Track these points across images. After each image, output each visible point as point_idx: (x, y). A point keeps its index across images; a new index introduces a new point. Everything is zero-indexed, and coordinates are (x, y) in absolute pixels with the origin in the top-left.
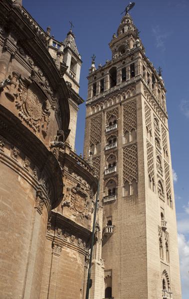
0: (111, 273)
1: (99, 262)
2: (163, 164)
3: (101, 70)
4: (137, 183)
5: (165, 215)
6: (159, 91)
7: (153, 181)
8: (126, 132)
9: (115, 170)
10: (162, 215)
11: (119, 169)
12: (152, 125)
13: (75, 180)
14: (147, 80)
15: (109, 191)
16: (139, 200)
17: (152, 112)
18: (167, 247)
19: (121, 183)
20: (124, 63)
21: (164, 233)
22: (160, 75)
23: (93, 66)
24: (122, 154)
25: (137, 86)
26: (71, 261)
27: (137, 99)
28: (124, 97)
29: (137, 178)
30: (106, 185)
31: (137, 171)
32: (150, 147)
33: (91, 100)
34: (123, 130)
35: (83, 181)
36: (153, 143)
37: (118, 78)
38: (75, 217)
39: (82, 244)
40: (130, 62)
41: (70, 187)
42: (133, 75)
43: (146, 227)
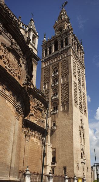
0: (55, 150)
1: (49, 145)
3: (49, 42)
4: (68, 104)
5: (83, 120)
6: (81, 54)
7: (77, 103)
8: (63, 77)
10: (81, 120)
11: (59, 96)
12: (77, 73)
13: (36, 102)
14: (74, 47)
15: (54, 108)
16: (70, 112)
17: (77, 65)
18: (84, 136)
19: (60, 104)
20: (62, 37)
21: (82, 130)
22: (81, 44)
23: (45, 39)
24: (61, 88)
25: (69, 51)
26: (35, 144)
27: (69, 58)
28: (62, 57)
29: (69, 101)
30: (53, 105)
31: (69, 97)
32: (75, 84)
33: (44, 59)
35: (40, 103)
36: (77, 82)
37: (58, 46)
38: (36, 122)
39: (40, 135)
40: (65, 37)
41: (34, 106)
42: (67, 44)
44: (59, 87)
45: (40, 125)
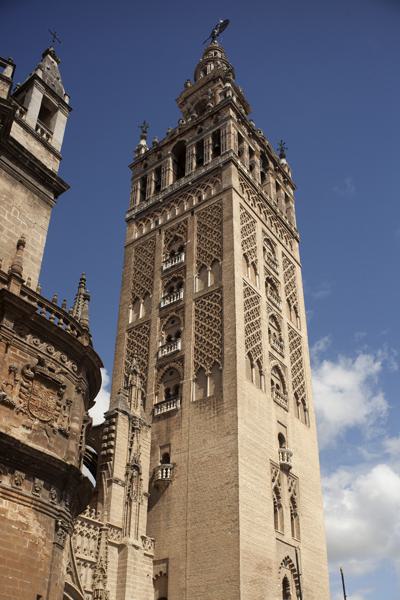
0: (167, 567)
1: (139, 543)
2: (285, 333)
3: (157, 149)
4: (221, 371)
5: (289, 439)
6: (278, 187)
7: (260, 367)
8: (202, 269)
9: (179, 348)
11: (187, 346)
12: (260, 252)
13: (33, 351)
14: (248, 163)
15: (167, 391)
16: (225, 406)
17: (259, 226)
19: (190, 373)
20: (201, 131)
21: (285, 476)
22: (282, 156)
23: (143, 142)
25: (224, 173)
26: (12, 530)
27: (225, 199)
28: (200, 198)
29: (222, 359)
30: (162, 380)
31: (222, 346)
33: (136, 211)
34: (195, 265)
35: (57, 355)
36: (261, 289)
37: (188, 162)
39: (45, 492)
40: (211, 129)
41: (19, 365)
42: (217, 152)
43: (237, 463)
44: (187, 309)
45: (49, 447)
